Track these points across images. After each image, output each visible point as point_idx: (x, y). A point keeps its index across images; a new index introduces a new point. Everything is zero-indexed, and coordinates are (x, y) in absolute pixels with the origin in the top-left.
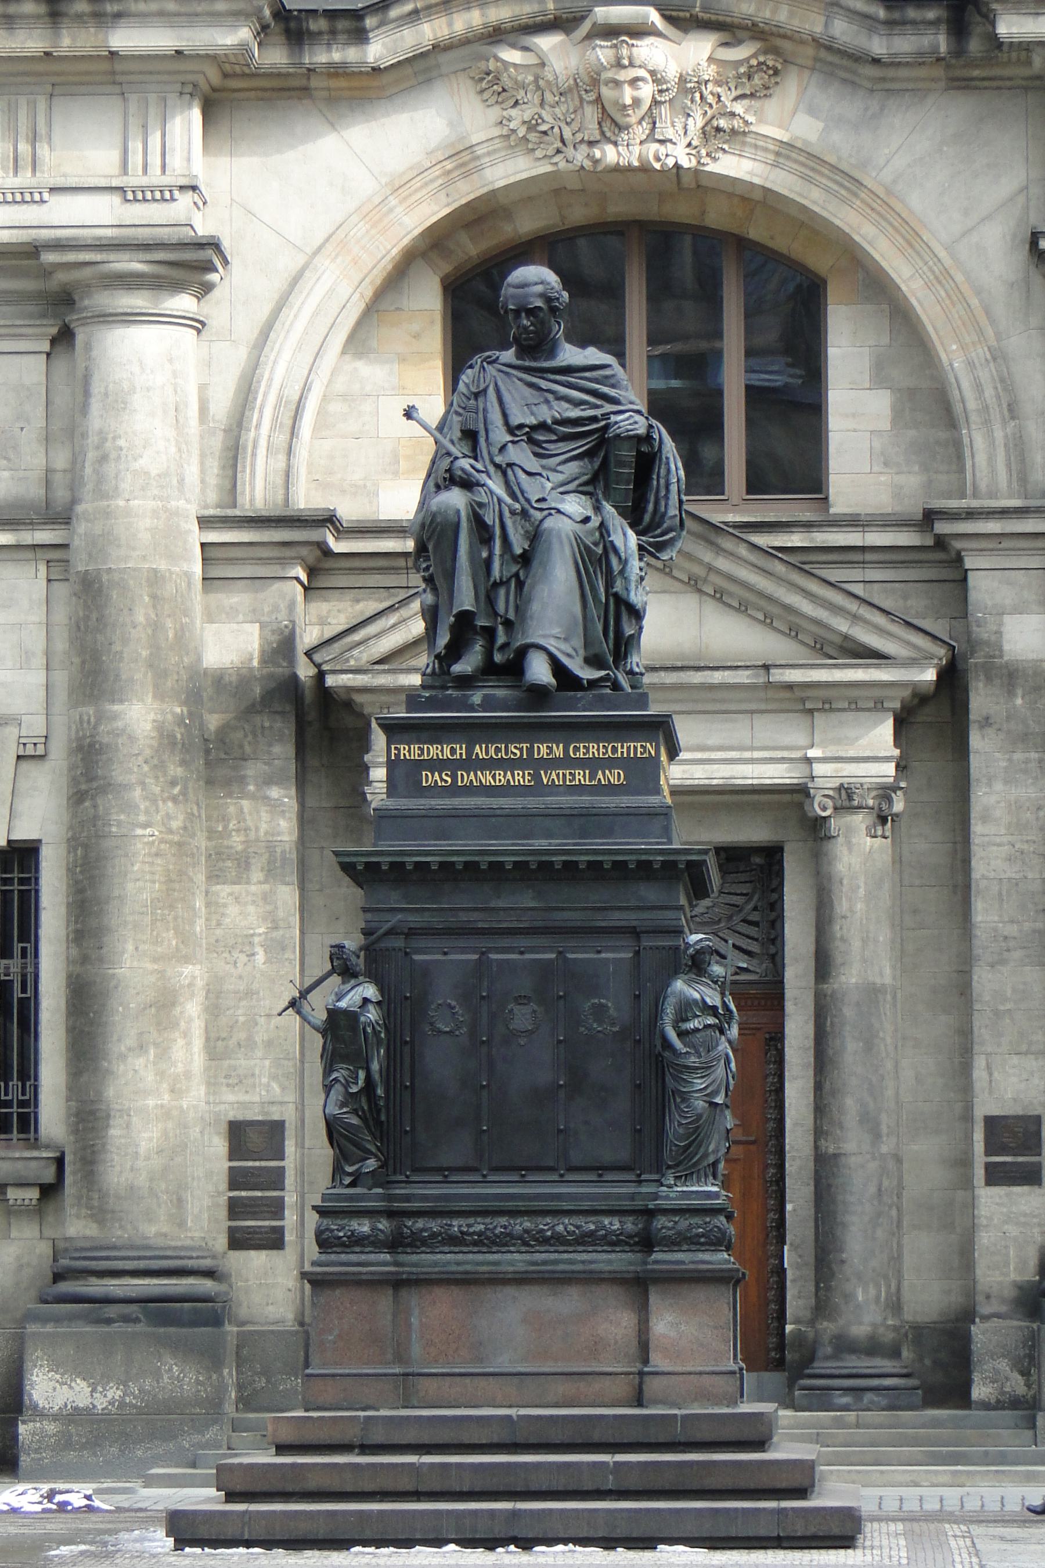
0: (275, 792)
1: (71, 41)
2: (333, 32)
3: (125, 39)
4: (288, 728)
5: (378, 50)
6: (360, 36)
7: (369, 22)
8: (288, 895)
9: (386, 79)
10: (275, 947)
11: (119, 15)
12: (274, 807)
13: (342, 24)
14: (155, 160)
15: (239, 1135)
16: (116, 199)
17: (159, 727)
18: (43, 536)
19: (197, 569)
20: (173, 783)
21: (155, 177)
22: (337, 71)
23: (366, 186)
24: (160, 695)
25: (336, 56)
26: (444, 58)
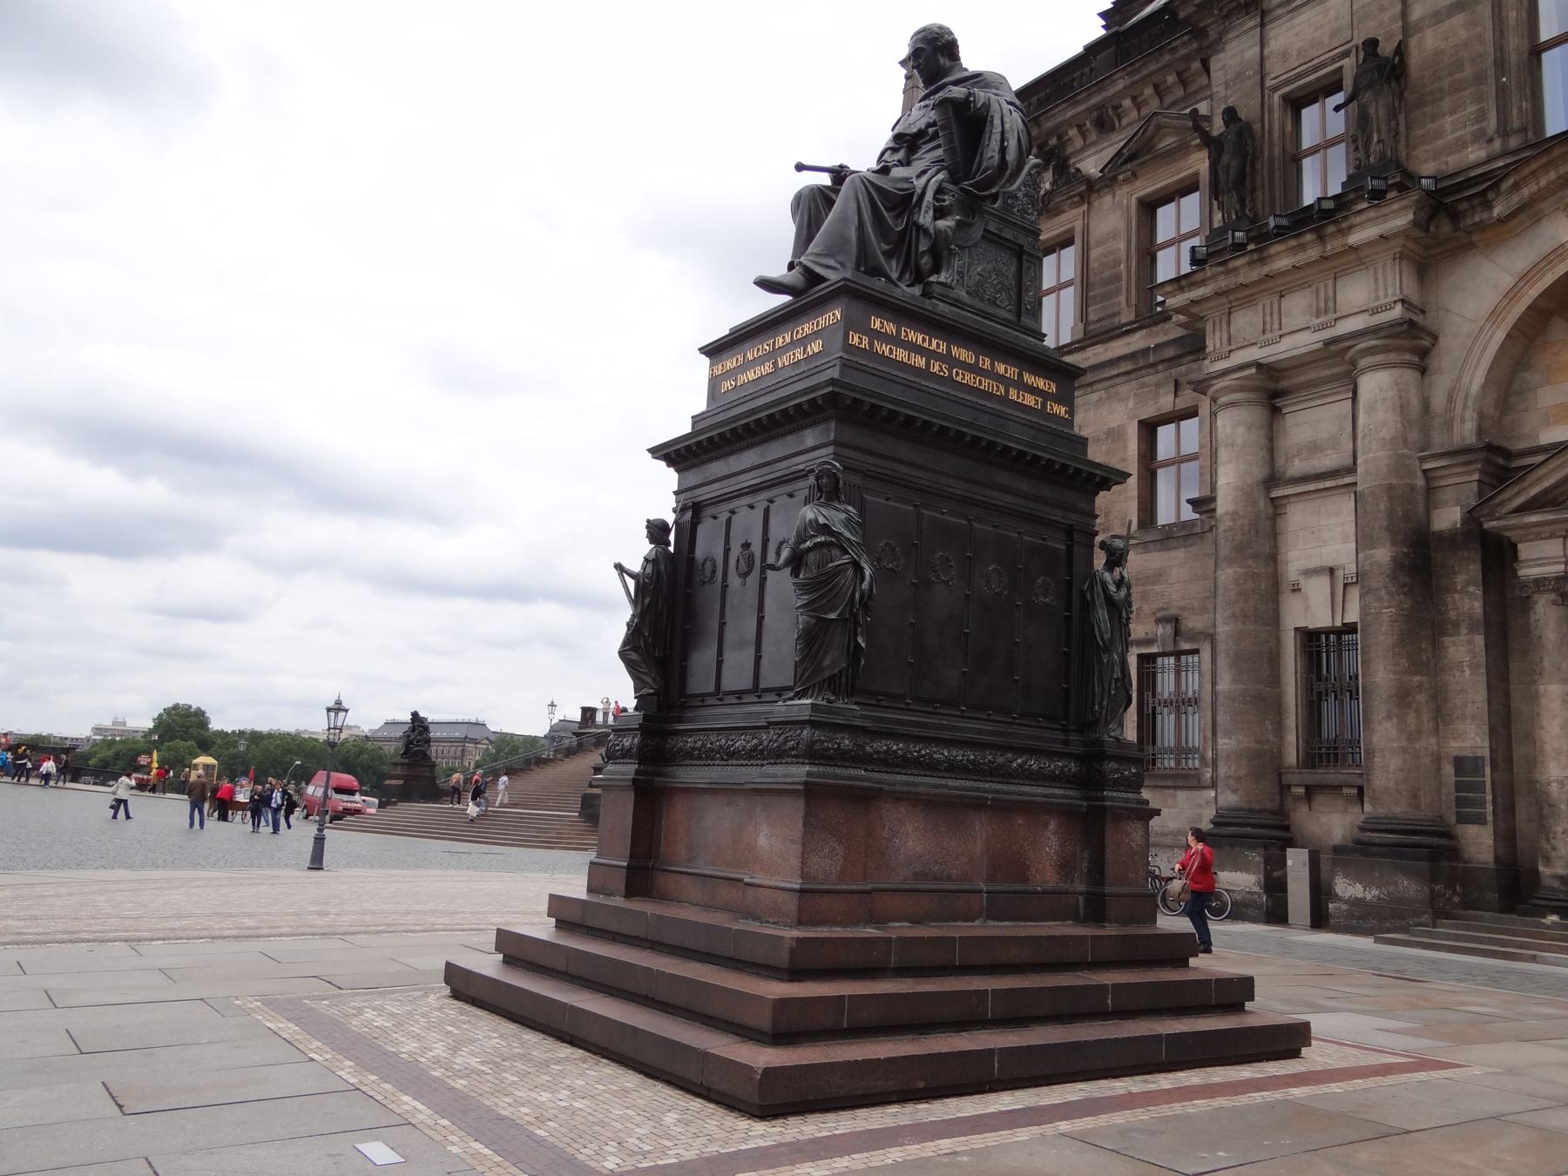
0: (1471, 589)
1: (1332, 246)
2: (1473, 208)
3: (1354, 238)
4: (1476, 555)
5: (1497, 211)
6: (1488, 206)
7: (1490, 196)
8: (1479, 640)
9: (1513, 223)
10: (1474, 667)
11: (1351, 227)
12: (1471, 596)
13: (1477, 201)
14: (1381, 293)
15: (1460, 763)
16: (1366, 315)
17: (1394, 559)
18: (1348, 480)
19: (1420, 482)
20: (1404, 585)
21: (1383, 301)
22: (1481, 227)
23: (1507, 281)
24: (1394, 543)
25: (1477, 219)
26: (1544, 205)
